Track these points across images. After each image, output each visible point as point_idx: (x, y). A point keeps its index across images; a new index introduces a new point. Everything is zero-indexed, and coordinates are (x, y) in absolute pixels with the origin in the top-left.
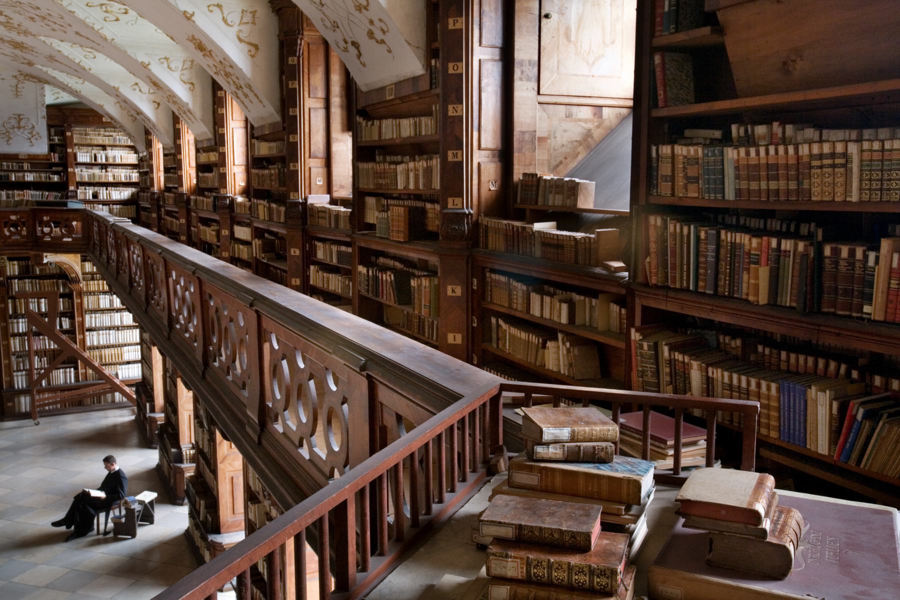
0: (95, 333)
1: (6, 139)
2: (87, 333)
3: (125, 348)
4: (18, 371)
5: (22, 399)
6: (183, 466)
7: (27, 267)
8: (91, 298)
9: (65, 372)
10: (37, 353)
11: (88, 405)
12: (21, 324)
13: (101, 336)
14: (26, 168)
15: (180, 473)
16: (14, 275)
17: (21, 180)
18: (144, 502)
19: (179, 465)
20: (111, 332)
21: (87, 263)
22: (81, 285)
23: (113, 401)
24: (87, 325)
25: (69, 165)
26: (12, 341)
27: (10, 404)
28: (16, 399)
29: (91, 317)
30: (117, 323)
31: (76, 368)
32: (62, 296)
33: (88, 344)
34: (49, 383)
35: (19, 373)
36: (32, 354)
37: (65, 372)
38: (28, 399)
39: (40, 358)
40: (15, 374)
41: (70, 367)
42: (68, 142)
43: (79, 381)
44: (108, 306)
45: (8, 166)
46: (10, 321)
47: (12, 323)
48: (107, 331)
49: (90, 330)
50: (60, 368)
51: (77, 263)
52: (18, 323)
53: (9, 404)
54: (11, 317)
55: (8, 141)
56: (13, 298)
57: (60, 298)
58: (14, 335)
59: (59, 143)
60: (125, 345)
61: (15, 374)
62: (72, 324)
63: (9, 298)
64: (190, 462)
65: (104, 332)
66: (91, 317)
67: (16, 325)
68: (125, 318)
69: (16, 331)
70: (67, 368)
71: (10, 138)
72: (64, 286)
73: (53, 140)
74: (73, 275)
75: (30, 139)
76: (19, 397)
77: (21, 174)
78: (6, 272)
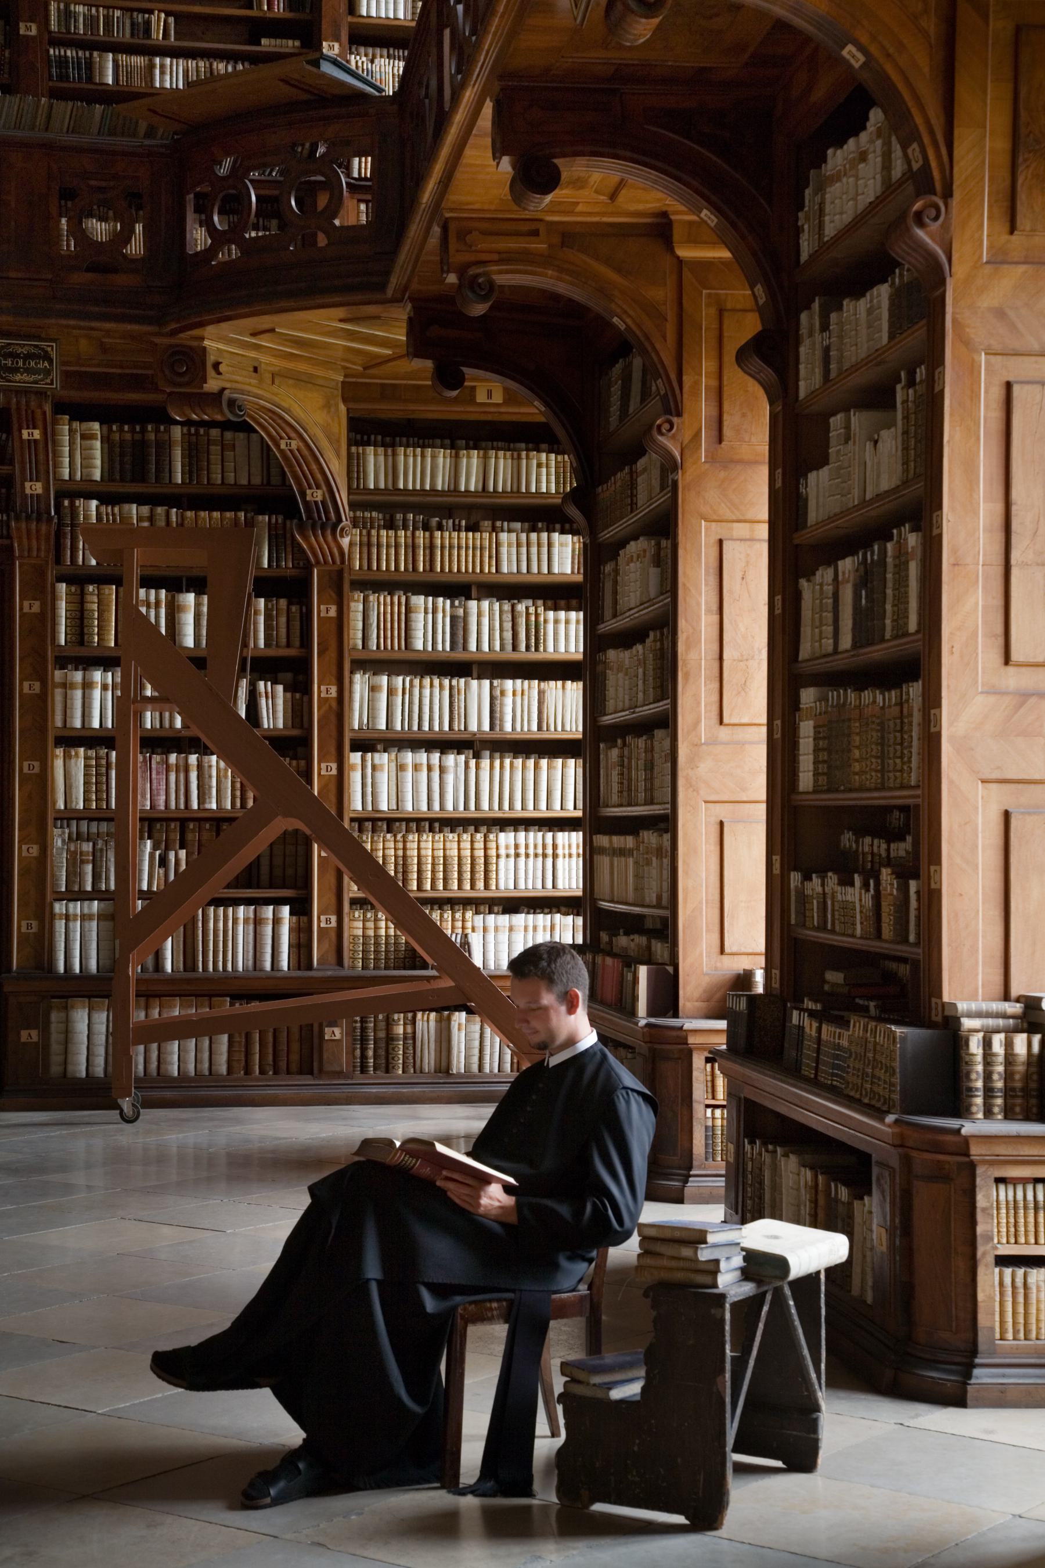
0: (383, 759)
2: (355, 758)
3: (506, 839)
4: (75, 895)
5: (81, 1018)
6: (968, 1128)
7: (140, 447)
8: (378, 601)
9: (258, 922)
10: (151, 823)
11: (339, 1074)
12: (97, 693)
13: (409, 774)
15: (940, 1176)
16: (88, 480)
17: (138, 83)
18: (780, 1264)
19: (952, 1123)
20: (451, 759)
21: (370, 450)
22: (345, 542)
23: (444, 1068)
24: (356, 719)
25: (326, 27)
26: (59, 764)
27: (29, 1036)
28: (55, 1016)
29: (373, 689)
30: (478, 722)
31: (301, 908)
32: (266, 587)
33: (356, 803)
35: (76, 908)
36: (133, 825)
37: (258, 922)
38: (101, 1018)
39: (164, 847)
40: (59, 908)
41: (278, 902)
43: (309, 967)
44: (443, 644)
45: (91, 22)
46: (58, 675)
47: (67, 686)
48: (436, 756)
49: (366, 745)
50: (236, 902)
51: (334, 442)
52: (87, 686)
53: (24, 1035)
54: (63, 662)
56: (79, 579)
57: (258, 596)
58: (70, 740)
61: (59, 908)
62: (299, 713)
63: (60, 580)
64: (1009, 1114)
65: (422, 757)
66: (373, 689)
67: (78, 694)
68: (509, 700)
70: (267, 902)
72: (279, 540)
74: (317, 495)
76: (66, 1008)
77: (138, 61)
78: (57, 465)
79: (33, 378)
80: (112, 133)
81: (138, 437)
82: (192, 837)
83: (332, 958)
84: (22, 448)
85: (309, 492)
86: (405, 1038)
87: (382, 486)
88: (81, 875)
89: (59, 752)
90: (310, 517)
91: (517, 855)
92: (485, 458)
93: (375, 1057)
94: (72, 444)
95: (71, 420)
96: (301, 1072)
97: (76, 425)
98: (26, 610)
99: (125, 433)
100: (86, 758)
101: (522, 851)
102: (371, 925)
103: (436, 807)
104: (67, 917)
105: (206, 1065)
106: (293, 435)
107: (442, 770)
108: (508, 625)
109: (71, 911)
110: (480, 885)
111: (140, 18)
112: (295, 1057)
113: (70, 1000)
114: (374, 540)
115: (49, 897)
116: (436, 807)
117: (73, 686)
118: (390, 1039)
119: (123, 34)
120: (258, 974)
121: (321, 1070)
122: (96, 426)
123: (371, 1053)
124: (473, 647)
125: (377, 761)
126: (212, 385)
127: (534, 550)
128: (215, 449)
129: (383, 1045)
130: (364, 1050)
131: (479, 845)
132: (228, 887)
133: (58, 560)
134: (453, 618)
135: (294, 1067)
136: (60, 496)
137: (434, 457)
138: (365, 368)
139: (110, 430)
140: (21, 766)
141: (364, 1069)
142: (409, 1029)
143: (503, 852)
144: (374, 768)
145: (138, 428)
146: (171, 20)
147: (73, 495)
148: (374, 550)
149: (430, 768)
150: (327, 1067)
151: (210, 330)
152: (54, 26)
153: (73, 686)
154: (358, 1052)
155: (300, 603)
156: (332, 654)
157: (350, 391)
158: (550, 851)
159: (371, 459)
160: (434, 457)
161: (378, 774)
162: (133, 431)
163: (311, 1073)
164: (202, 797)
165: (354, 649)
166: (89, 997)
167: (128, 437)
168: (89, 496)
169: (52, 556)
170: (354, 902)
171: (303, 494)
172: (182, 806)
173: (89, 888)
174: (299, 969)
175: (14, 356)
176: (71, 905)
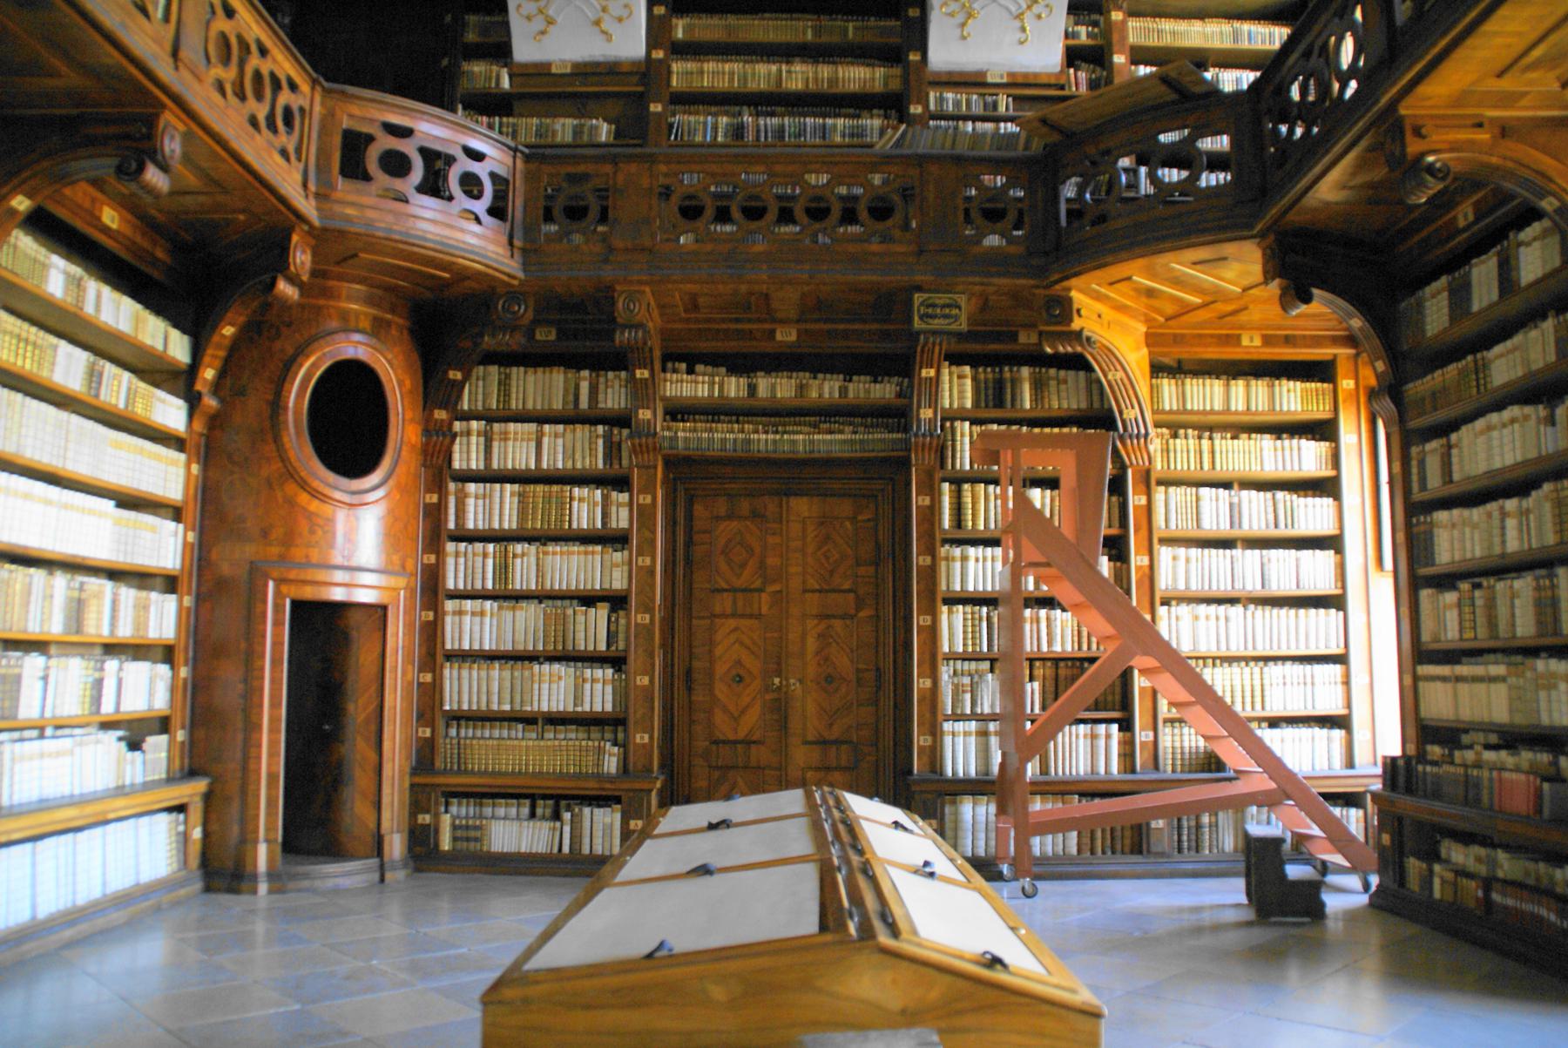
1: (960, 18)
3: (1274, 670)
4: (957, 717)
9: (1094, 737)
11: (1162, 854)
12: (971, 564)
14: (1002, 109)
16: (962, 408)
24: (1164, 582)
26: (944, 617)
28: (948, 809)
31: (1126, 725)
34: (1044, 770)
35: (960, 726)
37: (1094, 737)
40: (947, 726)
42: (1115, 37)
43: (1133, 771)
45: (957, 104)
52: (964, 559)
55: (963, 25)
56: (958, 481)
59: (1090, 42)
60: (1275, 659)
61: (947, 726)
63: (944, 480)
67: (958, 565)
69: (958, 588)
71: (970, 16)
73: (1075, 35)
75: (1019, 17)
76: (954, 803)
79: (947, 321)
80: (999, 149)
81: (997, 376)
82: (1039, 672)
83: (1150, 764)
84: (920, 384)
85: (1125, 411)
86: (1210, 826)
87: (1175, 408)
88: (963, 701)
89: (945, 609)
90: (1125, 429)
91: (1285, 684)
92: (1248, 386)
93: (1189, 840)
94: (951, 382)
95: (950, 365)
96: (1132, 852)
97: (954, 368)
98: (920, 503)
99: (987, 373)
100: (964, 613)
101: (1288, 681)
102: (1177, 738)
103: (1223, 647)
104: (953, 734)
105: (1061, 847)
106: (1119, 367)
107: (1227, 619)
108: (1271, 509)
109: (956, 729)
110: (1258, 706)
111: (989, 99)
112: (1127, 842)
113: (958, 798)
114: (1171, 447)
115: (940, 718)
116: (1223, 647)
117: (953, 559)
118: (1199, 826)
119: (977, 109)
120: (1095, 777)
121: (1149, 852)
122: (967, 369)
123: (1185, 838)
124: (1246, 526)
125: (1179, 614)
126: (1076, 324)
127: (1287, 452)
128: (1053, 383)
129: (1194, 830)
130: (1180, 835)
131: (1257, 676)
132: (1088, 709)
133: (943, 465)
134: (1231, 505)
135: (1127, 849)
136: (943, 420)
137: (1211, 386)
138: (1167, 320)
139: (977, 373)
140: (919, 620)
141: (1180, 850)
142: (1213, 819)
143: (1274, 682)
144: (1177, 618)
145: (997, 370)
146: (1010, 99)
147: (953, 420)
148: (1172, 455)
149: (1217, 618)
150: (1154, 849)
151: (1074, 282)
152: (932, 107)
153: (953, 559)
154: (1176, 837)
155: (1119, 495)
156: (1144, 532)
157: (1151, 340)
158: (1309, 680)
159: (1166, 388)
160: (1211, 386)
161: (1180, 623)
162: (993, 372)
163: (1140, 852)
164: (1050, 643)
165: (1160, 528)
166: (973, 794)
167: (990, 376)
168: (963, 420)
169: (938, 464)
170: (1166, 721)
171: (1121, 413)
172: (1035, 649)
173: (968, 711)
174: (1125, 772)
175: (933, 306)
176: (956, 724)
